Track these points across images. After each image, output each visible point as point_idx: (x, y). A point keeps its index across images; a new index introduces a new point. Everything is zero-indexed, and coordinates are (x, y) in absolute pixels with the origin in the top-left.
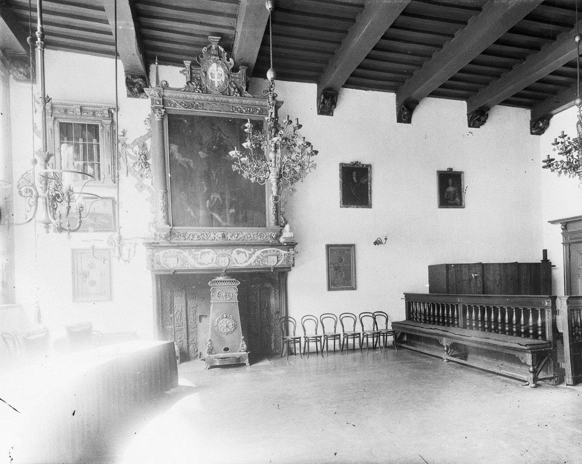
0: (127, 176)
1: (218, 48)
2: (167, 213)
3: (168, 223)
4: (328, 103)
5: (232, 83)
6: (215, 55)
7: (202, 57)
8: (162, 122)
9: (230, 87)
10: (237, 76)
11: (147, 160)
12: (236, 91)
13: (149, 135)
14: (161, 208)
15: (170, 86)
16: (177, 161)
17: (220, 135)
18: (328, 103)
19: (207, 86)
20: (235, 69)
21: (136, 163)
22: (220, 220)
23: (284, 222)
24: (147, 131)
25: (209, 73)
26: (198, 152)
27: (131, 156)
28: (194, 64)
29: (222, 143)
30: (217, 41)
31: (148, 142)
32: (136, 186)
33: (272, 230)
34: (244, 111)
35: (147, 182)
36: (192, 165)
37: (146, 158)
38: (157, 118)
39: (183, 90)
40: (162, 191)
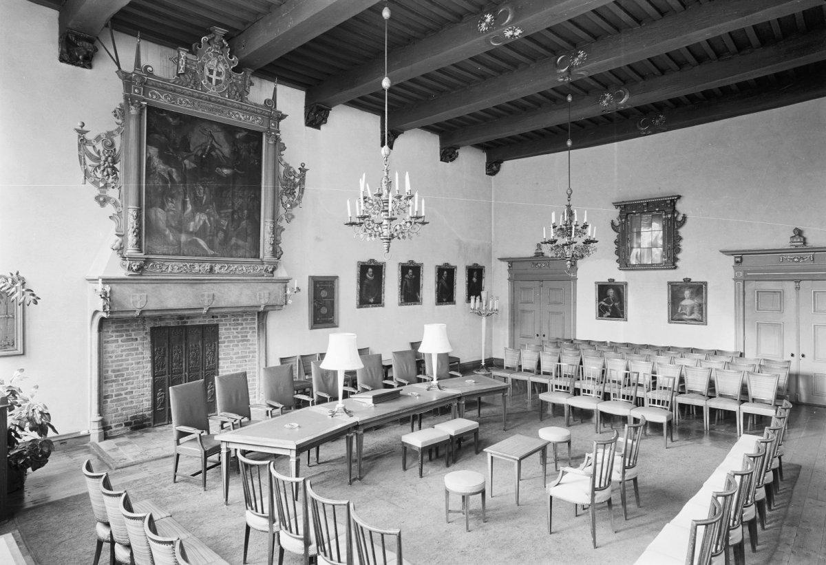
1: (222, 41)
3: (140, 251)
4: (316, 117)
6: (217, 49)
8: (140, 115)
10: (240, 77)
12: (238, 94)
18: (316, 117)
19: (203, 82)
21: (99, 166)
25: (206, 68)
26: (184, 159)
27: (91, 156)
29: (213, 153)
31: (118, 140)
32: (97, 198)
33: (269, 263)
34: (242, 118)
35: (113, 193)
36: (174, 176)
37: (114, 162)
38: (133, 111)
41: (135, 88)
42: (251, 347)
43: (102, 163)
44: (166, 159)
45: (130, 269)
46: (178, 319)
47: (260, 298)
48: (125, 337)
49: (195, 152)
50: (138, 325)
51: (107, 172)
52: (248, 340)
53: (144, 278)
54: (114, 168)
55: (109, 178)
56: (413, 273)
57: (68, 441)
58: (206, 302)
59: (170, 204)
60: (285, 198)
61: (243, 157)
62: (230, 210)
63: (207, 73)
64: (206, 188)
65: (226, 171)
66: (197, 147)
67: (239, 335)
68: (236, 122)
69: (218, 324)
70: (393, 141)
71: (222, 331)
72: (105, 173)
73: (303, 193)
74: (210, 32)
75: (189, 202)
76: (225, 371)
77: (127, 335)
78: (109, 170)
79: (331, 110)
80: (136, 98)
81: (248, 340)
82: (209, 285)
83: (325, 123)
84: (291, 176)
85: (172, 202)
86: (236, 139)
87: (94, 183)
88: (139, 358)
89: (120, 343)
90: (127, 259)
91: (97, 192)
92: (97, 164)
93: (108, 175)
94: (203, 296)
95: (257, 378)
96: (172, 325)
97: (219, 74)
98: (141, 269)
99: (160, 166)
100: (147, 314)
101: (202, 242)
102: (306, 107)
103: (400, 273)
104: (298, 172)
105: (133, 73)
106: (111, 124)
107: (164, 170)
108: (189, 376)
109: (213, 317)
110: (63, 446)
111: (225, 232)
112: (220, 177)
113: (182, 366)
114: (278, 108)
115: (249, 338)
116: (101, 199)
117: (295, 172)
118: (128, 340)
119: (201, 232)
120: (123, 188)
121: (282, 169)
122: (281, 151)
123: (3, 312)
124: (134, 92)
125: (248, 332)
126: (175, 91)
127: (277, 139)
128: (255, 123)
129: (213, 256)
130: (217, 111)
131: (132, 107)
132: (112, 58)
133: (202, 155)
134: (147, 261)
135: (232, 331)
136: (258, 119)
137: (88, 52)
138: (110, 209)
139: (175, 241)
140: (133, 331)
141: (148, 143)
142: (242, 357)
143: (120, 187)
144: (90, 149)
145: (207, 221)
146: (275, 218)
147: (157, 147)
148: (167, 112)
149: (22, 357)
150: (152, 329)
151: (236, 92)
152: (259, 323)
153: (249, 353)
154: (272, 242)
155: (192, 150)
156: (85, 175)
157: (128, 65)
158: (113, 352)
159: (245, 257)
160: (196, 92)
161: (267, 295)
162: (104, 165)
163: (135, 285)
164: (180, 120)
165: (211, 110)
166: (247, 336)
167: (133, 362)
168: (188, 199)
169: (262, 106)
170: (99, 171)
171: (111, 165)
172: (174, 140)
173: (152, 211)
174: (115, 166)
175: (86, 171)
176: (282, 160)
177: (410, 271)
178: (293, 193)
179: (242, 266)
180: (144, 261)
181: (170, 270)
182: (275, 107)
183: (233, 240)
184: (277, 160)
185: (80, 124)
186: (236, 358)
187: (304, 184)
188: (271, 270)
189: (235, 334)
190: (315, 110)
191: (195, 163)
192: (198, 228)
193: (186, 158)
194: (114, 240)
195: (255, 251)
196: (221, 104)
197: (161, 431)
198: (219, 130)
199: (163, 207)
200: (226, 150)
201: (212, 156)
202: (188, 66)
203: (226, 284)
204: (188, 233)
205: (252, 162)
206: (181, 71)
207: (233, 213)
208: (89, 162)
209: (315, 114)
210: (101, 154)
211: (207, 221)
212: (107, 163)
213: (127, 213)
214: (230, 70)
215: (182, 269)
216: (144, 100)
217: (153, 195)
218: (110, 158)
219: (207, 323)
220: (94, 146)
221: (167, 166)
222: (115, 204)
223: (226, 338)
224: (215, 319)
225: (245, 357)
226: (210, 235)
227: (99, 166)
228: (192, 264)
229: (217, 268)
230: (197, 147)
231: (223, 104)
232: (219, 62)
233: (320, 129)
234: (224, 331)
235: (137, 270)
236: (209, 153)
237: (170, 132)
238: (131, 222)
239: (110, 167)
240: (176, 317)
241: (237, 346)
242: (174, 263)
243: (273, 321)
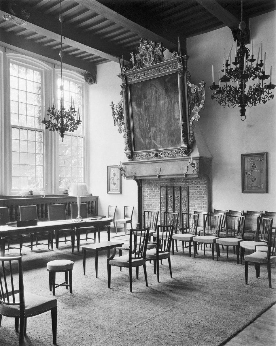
12: (158, 60)
48: (150, 190)
77: (151, 189)
89: (149, 192)
125: (203, 192)
135: (195, 190)
140: (154, 187)
158: (146, 196)
186: (198, 207)
203: (166, 163)
223: (192, 194)
228: (149, 153)
234: (191, 190)
241: (197, 199)
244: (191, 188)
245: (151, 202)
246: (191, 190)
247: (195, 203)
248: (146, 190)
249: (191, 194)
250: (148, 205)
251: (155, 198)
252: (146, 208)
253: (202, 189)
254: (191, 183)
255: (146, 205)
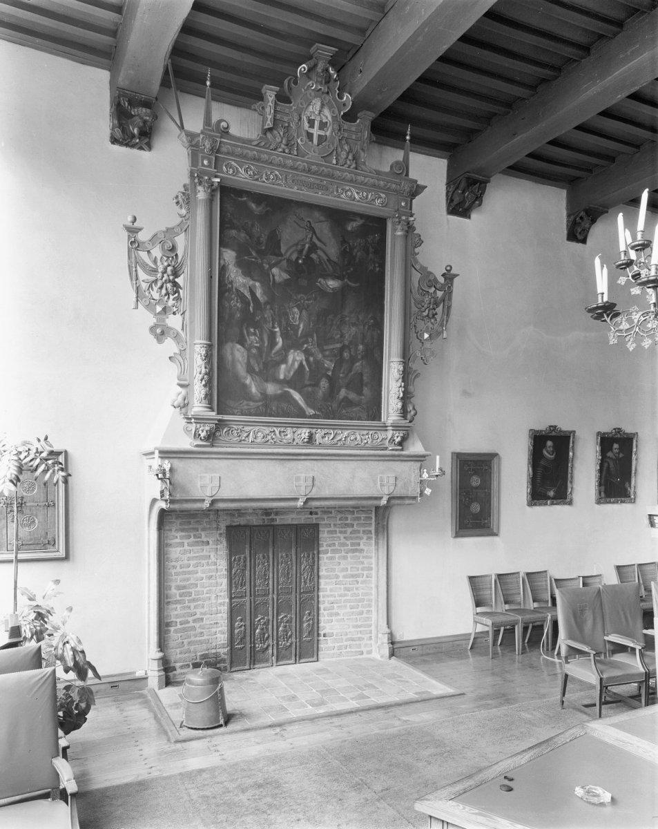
0: (137, 308)
1: (327, 70)
2: (211, 388)
3: (211, 409)
4: (465, 197)
5: (344, 142)
6: (321, 84)
7: (296, 83)
8: (211, 201)
9: (339, 149)
10: (353, 129)
11: (177, 277)
12: (350, 157)
13: (185, 227)
14: (201, 376)
15: (232, 131)
16: (231, 283)
17: (311, 238)
19: (299, 141)
20: (350, 117)
21: (156, 281)
22: (301, 402)
23: (413, 413)
24: (179, 220)
25: (304, 118)
26: (271, 266)
27: (144, 266)
28: (282, 98)
29: (314, 256)
30: (327, 55)
31: (181, 241)
32: (152, 329)
33: (396, 427)
35: (174, 321)
36: (259, 293)
37: (176, 274)
38: (202, 194)
39: (255, 143)
40: (205, 342)
41: (203, 158)
42: (366, 561)
43: (159, 275)
44: (247, 268)
45: (197, 435)
46: (262, 515)
47: (382, 485)
48: (192, 539)
49: (289, 253)
50: (210, 523)
51: (166, 289)
52: (362, 550)
53: (215, 449)
54: (175, 284)
55: (169, 298)
56: (621, 449)
57: (121, 685)
58: (303, 489)
59: (253, 337)
60: (421, 325)
61: (357, 260)
62: (338, 345)
63: (306, 125)
64: (304, 312)
65: (332, 284)
66: (291, 247)
67: (348, 542)
68: (349, 204)
69: (318, 524)
70: (589, 229)
71: (324, 535)
72: (164, 291)
73: (448, 315)
74: (311, 58)
75: (278, 334)
76: (328, 596)
77: (195, 536)
78: (169, 285)
79: (489, 182)
80: (205, 173)
81: (362, 550)
82: (308, 463)
83: (480, 205)
84: (430, 287)
85: (255, 334)
86: (347, 231)
87: (150, 307)
88: (210, 571)
89: (186, 547)
90: (193, 420)
91: (152, 320)
92: (154, 278)
93: (167, 294)
94: (298, 479)
95: (373, 609)
96: (255, 523)
97: (323, 126)
98: (211, 437)
99: (238, 279)
100: (221, 505)
101: (297, 396)
102: (448, 184)
103: (598, 448)
104: (442, 280)
105: (202, 133)
106: (171, 216)
107: (244, 285)
108: (278, 600)
109: (311, 513)
110: (114, 690)
111: (330, 379)
112: (323, 293)
113: (268, 584)
114: (412, 175)
115: (362, 547)
116: (159, 331)
117: (436, 280)
118: (196, 544)
119: (296, 381)
120: (187, 314)
121: (416, 276)
122: (415, 247)
123: (42, 499)
124: (203, 165)
125: (361, 538)
126: (258, 160)
127: (410, 228)
128: (376, 204)
129: (314, 416)
130: (320, 187)
131: (200, 188)
132: (177, 124)
133: (298, 259)
134: (220, 424)
135: (339, 535)
136: (380, 197)
137: (145, 122)
138: (170, 346)
139: (259, 395)
140: (204, 529)
141: (222, 244)
142: (352, 576)
143: (183, 313)
144: (143, 255)
145: (304, 363)
146: (406, 356)
147: (234, 250)
148: (248, 193)
149: (65, 565)
150: (229, 528)
151: (348, 154)
152: (377, 524)
153: (363, 569)
154: (401, 395)
155: (283, 251)
156: (137, 297)
157: (195, 124)
158: (177, 560)
159: (359, 419)
160: (289, 158)
161: (392, 481)
162: (162, 279)
163: (203, 461)
164: (267, 206)
165: (310, 186)
166: (359, 544)
167: (204, 575)
168: (277, 330)
169: (386, 174)
170: (155, 289)
171: (171, 278)
172: (259, 238)
173: (228, 347)
174: (176, 280)
175: (138, 290)
176: (417, 262)
177: (616, 446)
178: (434, 315)
179: (354, 434)
180: (216, 424)
181: (251, 438)
182: (407, 175)
183: (343, 393)
184: (409, 262)
185: (130, 219)
186: (344, 577)
187: (450, 299)
188: (399, 439)
189: (343, 540)
190: (463, 185)
191: (286, 271)
192: (292, 373)
193: (275, 265)
194: (174, 393)
195: (373, 411)
196: (325, 176)
197: (240, 681)
198: (322, 218)
199: (242, 342)
200: (332, 249)
201: (312, 259)
202: (278, 116)
203: (332, 462)
204: (276, 380)
205: (371, 268)
206: (269, 124)
207: (342, 350)
208: (142, 275)
209: (464, 192)
210: (159, 263)
211: (304, 363)
212: (165, 275)
213: (192, 351)
214: (339, 118)
215: (269, 437)
216: (216, 177)
217: (228, 321)
218: (169, 269)
219: (303, 522)
220: (149, 252)
221: (248, 278)
222: (177, 337)
223: (329, 545)
224: (314, 516)
225: (357, 576)
226: (310, 385)
227: (156, 281)
229: (318, 436)
230: (291, 247)
231: (328, 176)
232: (322, 106)
233: (469, 218)
234: (326, 535)
235: (207, 438)
236: (308, 256)
237: (253, 225)
238: (199, 365)
239: (170, 281)
240: (260, 512)
241: (345, 558)
242: (257, 428)
243: (397, 521)
244: (326, 530)
245: (195, 576)
246: (326, 535)
247: (337, 567)
248: (178, 540)
249: (325, 544)
250: (184, 587)
251: (208, 564)
252: (178, 598)
253: (359, 532)
254: (325, 517)
255: (178, 588)
